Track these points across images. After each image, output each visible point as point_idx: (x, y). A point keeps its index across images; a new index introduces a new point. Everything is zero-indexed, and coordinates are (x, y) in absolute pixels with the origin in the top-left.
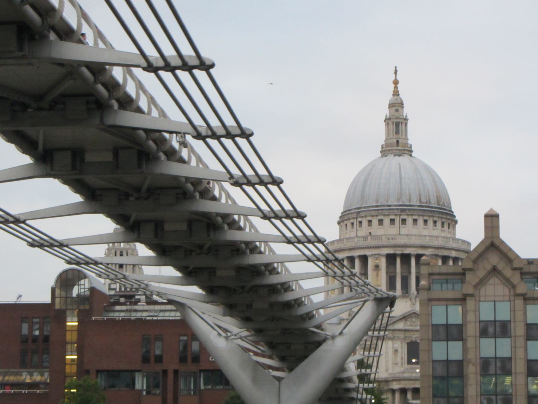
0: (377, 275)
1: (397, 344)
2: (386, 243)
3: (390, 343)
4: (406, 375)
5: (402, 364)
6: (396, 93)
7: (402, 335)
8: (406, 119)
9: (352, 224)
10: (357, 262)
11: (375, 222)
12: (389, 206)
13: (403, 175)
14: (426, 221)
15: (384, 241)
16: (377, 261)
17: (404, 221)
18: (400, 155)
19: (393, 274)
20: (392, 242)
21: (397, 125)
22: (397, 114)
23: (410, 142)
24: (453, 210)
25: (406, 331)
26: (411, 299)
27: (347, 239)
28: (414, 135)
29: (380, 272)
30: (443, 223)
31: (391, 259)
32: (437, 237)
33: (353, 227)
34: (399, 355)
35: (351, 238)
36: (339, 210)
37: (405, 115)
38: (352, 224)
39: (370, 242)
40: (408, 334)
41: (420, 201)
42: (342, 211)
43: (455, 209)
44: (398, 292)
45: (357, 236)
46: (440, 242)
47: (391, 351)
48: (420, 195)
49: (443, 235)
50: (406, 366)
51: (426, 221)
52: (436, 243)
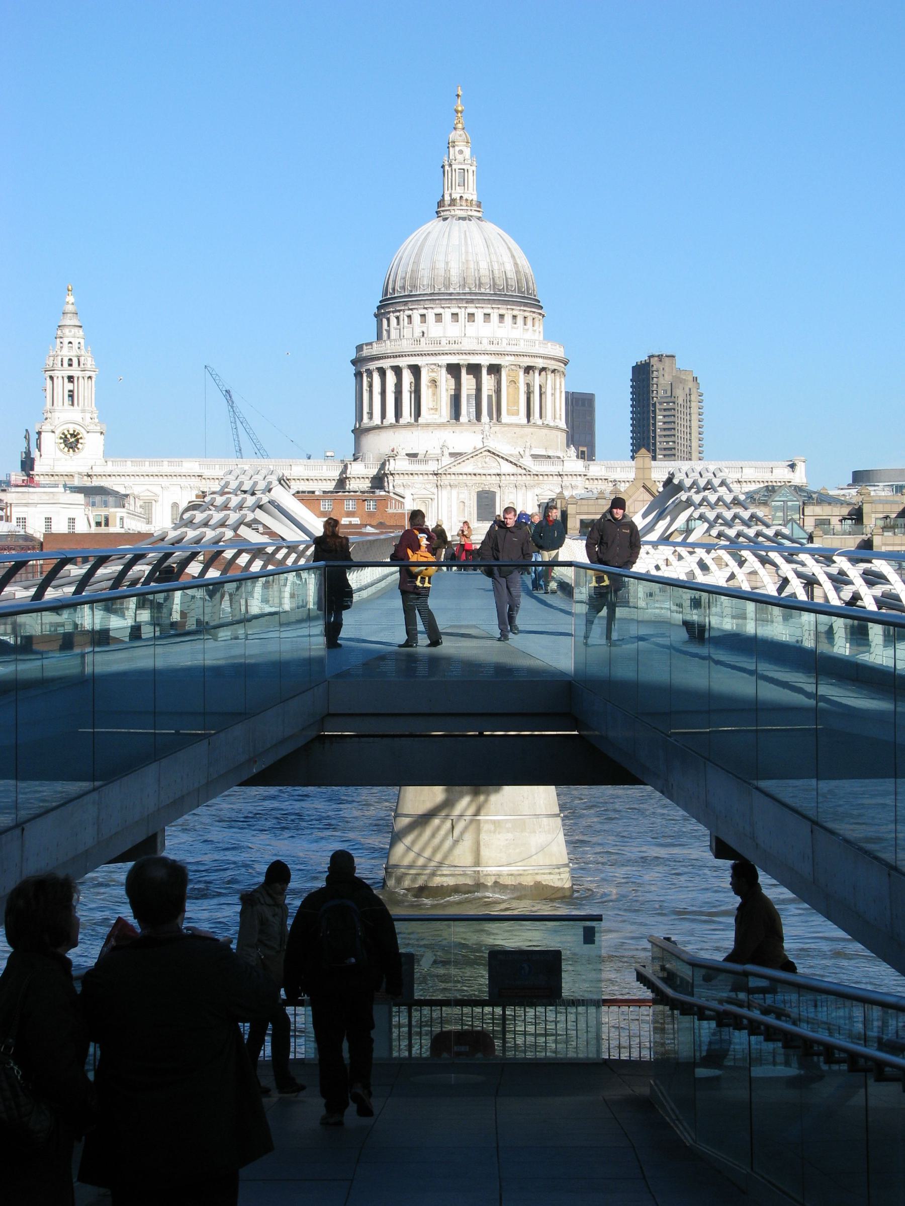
0: (434, 394)
2: (447, 348)
3: (454, 492)
12: (451, 294)
13: (470, 250)
14: (502, 316)
16: (434, 375)
17: (471, 316)
18: (464, 219)
20: (456, 347)
29: (438, 389)
31: (454, 370)
39: (424, 346)
46: (522, 348)
48: (493, 279)
51: (502, 316)
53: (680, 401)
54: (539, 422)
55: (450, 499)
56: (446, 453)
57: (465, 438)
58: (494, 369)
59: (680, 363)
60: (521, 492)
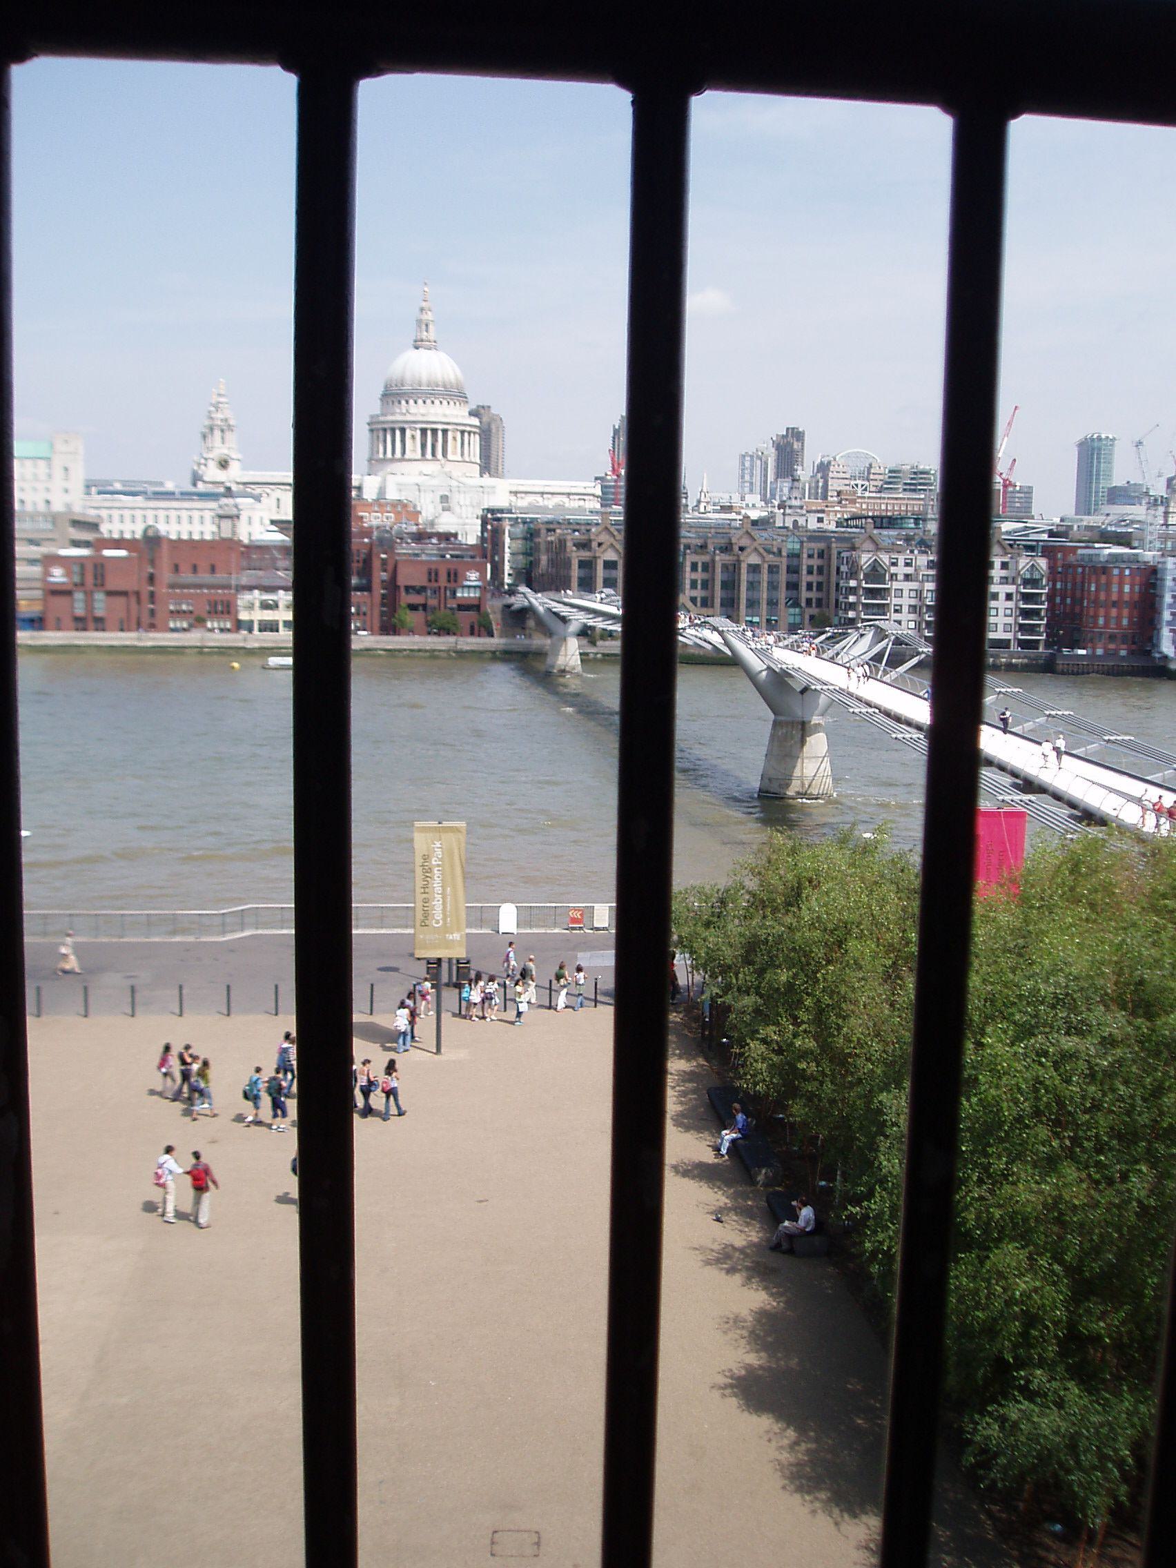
10: (398, 433)
11: (411, 402)
15: (421, 419)
20: (425, 419)
22: (424, 317)
31: (424, 431)
36: (381, 390)
39: (409, 418)
44: (429, 456)
59: (493, 411)
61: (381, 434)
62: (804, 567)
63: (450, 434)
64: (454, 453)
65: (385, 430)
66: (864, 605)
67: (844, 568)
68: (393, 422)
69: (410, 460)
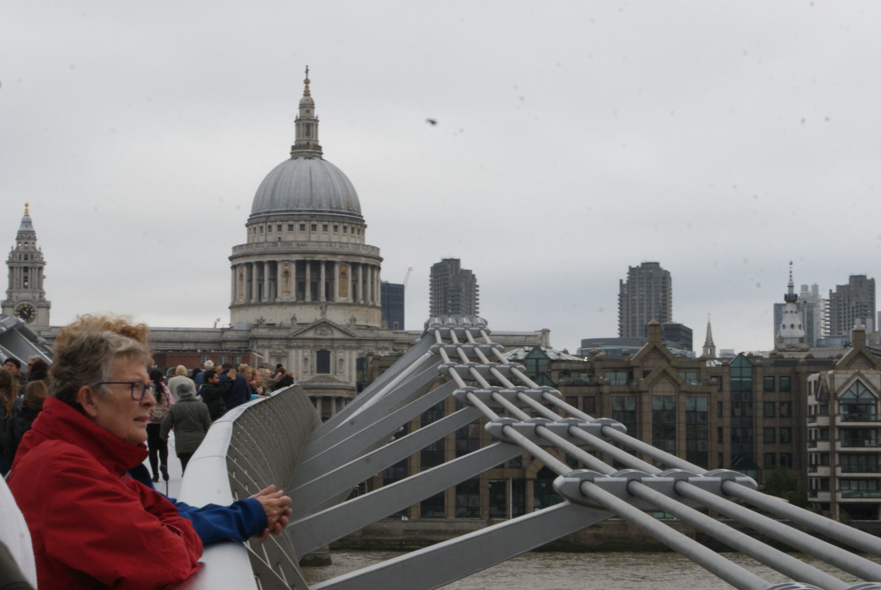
0: (287, 281)
1: (307, 353)
3: (300, 351)
4: (316, 384)
5: (312, 373)
6: (307, 93)
7: (312, 344)
8: (317, 121)
9: (261, 228)
10: (266, 269)
11: (285, 227)
12: (300, 211)
13: (313, 180)
17: (314, 227)
18: (310, 158)
19: (302, 280)
20: (302, 249)
21: (308, 126)
22: (307, 115)
23: (320, 144)
24: (363, 214)
25: (316, 339)
26: (321, 308)
27: (257, 244)
28: (324, 137)
30: (353, 229)
32: (347, 244)
33: (262, 231)
34: (309, 363)
35: (260, 243)
36: (246, 212)
37: (315, 115)
38: (261, 228)
39: (280, 247)
40: (318, 343)
41: (331, 207)
42: (250, 213)
43: (366, 213)
45: (266, 241)
46: (350, 249)
47: (301, 359)
48: (330, 201)
49: (352, 241)
50: (316, 374)
51: (336, 227)
52: (345, 250)
53: (464, 290)
54: (362, 302)
55: (297, 356)
56: (295, 323)
57: (308, 314)
58: (330, 265)
59: (464, 266)
60: (347, 353)
61: (245, 271)
62: (760, 405)
63: (337, 269)
64: (343, 294)
65: (249, 265)
66: (841, 454)
67: (812, 400)
68: (260, 254)
69: (282, 304)
